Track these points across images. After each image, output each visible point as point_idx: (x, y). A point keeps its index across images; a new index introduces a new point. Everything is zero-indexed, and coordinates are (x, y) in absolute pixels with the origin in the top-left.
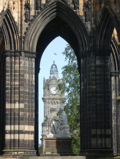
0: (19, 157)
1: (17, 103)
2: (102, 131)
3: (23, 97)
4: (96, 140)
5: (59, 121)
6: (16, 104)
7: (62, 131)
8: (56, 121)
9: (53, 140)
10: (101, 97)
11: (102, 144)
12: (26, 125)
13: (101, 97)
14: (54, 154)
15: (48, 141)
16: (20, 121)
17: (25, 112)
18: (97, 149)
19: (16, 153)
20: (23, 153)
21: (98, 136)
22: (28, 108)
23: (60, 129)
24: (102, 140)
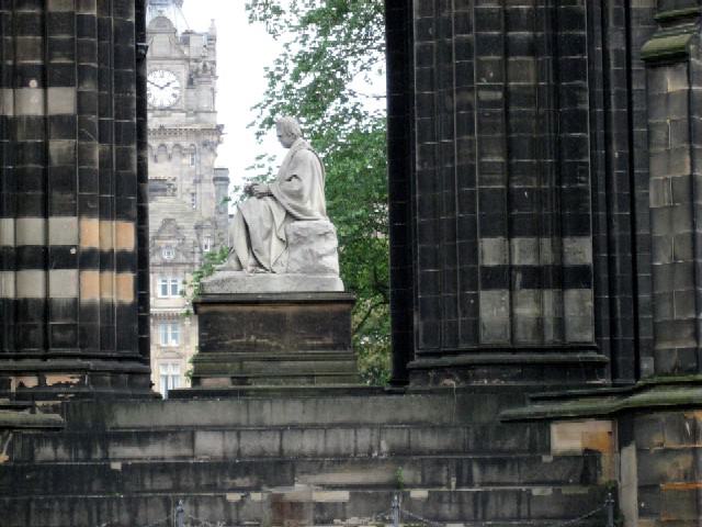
0: (51, 403)
1: (33, 83)
2: (538, 249)
3: (70, 49)
4: (506, 298)
5: (275, 199)
6: (25, 90)
7: (297, 254)
8: (261, 196)
9: (240, 308)
10: (532, 49)
11: (540, 324)
12: (90, 214)
13: (532, 49)
14: (253, 386)
15: (215, 313)
16: (56, 196)
17: (82, 136)
18: (514, 351)
19: (31, 382)
20: (76, 381)
21: (519, 277)
22: (100, 115)
23: (285, 242)
24: (539, 302)
